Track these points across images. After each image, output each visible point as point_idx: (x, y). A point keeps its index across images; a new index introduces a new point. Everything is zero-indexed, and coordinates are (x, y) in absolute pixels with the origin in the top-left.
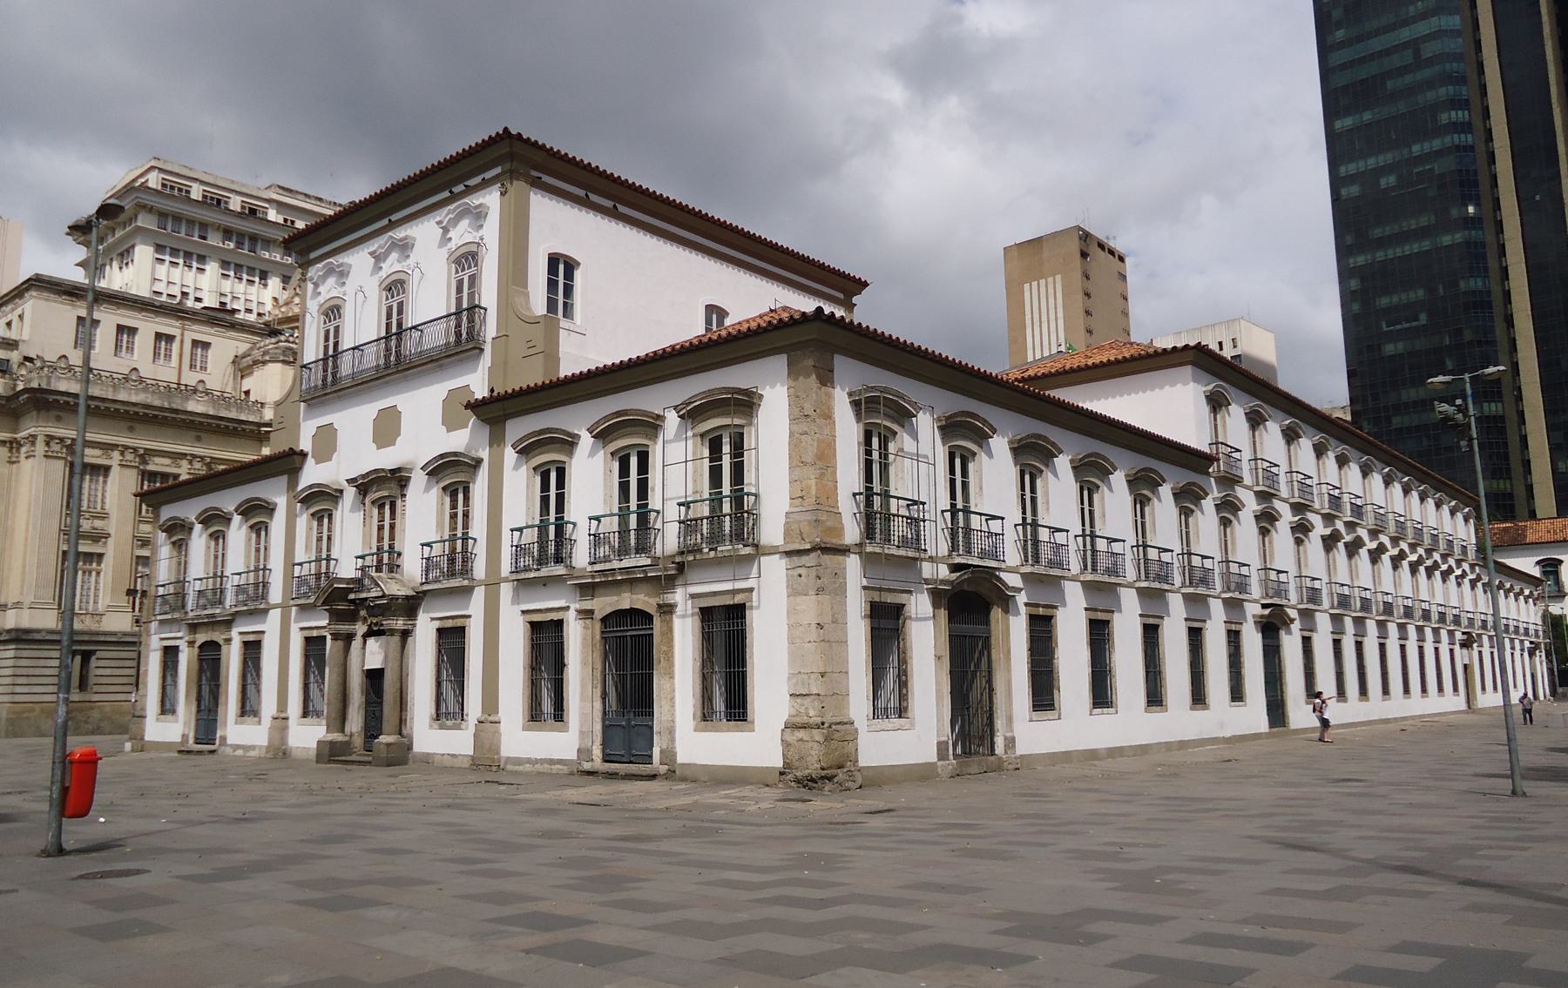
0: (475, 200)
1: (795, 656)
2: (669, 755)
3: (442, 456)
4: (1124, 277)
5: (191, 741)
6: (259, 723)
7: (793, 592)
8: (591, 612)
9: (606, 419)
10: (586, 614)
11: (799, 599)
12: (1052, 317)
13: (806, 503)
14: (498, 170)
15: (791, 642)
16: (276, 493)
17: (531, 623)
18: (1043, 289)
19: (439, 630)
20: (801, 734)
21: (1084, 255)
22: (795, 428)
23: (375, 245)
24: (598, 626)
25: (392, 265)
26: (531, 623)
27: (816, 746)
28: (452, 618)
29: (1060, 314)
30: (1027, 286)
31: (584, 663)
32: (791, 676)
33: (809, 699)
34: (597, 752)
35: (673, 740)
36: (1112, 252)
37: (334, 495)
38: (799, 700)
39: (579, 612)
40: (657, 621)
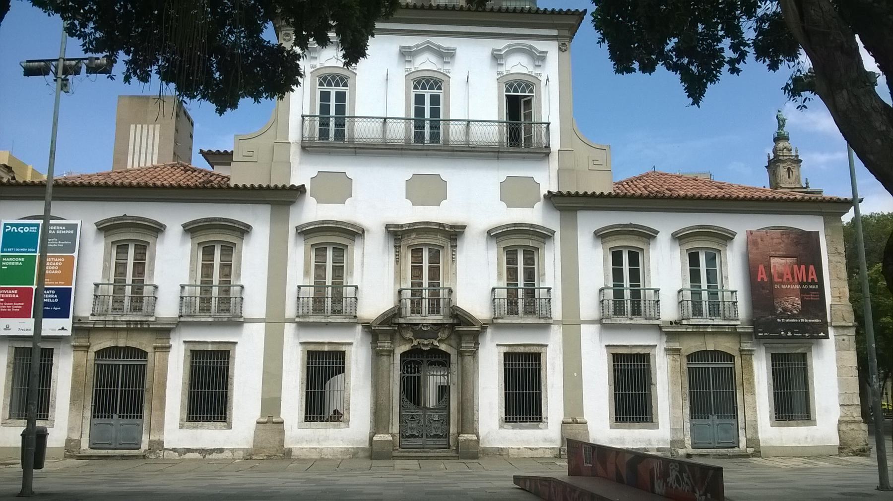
0: (540, 46)
1: (842, 383)
2: (753, 442)
3: (515, 225)
4: (191, 136)
5: (85, 445)
6: (229, 427)
7: (839, 349)
8: (679, 350)
9: (684, 230)
10: (671, 351)
11: (844, 353)
12: (149, 151)
13: (843, 300)
14: (555, 32)
15: (840, 375)
16: (258, 219)
17: (614, 355)
18: (151, 131)
19: (507, 355)
20: (853, 426)
21: (177, 116)
22: (832, 258)
23: (412, 42)
24: (685, 360)
25: (426, 63)
26: (614, 355)
27: (862, 432)
28: (525, 345)
29: (156, 151)
30: (132, 127)
31: (673, 383)
32: (840, 395)
33: (853, 407)
34: (688, 442)
35: (757, 432)
36: (189, 118)
37: (354, 233)
38: (846, 408)
39: (666, 350)
40: (738, 360)
